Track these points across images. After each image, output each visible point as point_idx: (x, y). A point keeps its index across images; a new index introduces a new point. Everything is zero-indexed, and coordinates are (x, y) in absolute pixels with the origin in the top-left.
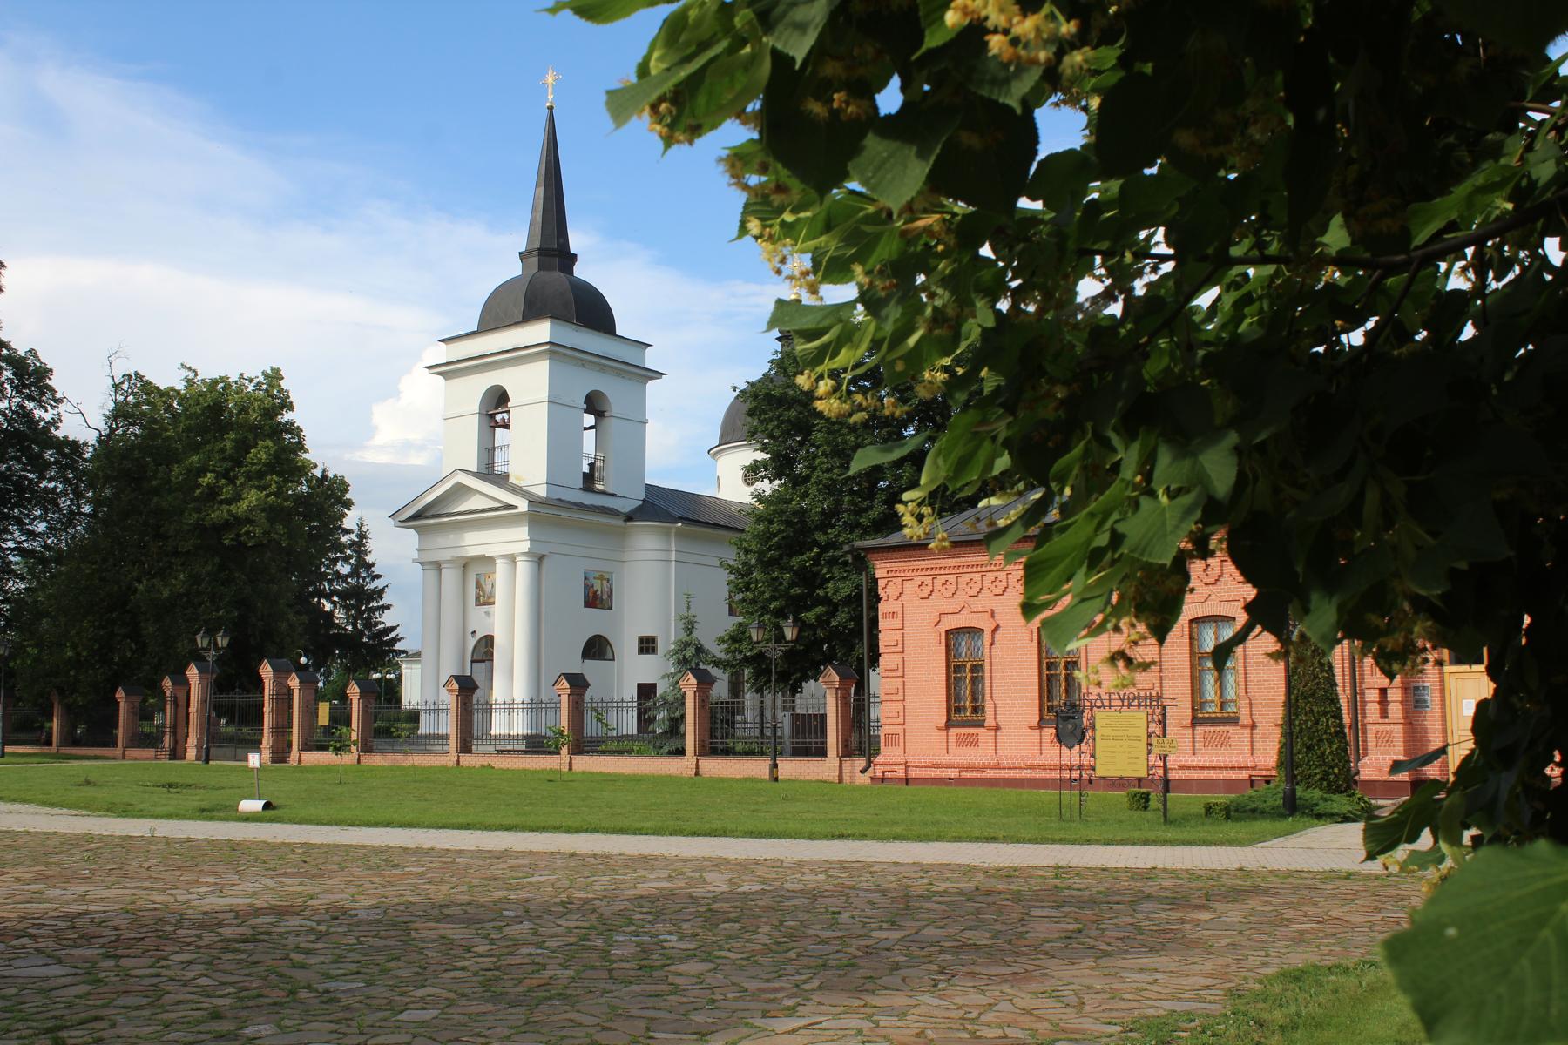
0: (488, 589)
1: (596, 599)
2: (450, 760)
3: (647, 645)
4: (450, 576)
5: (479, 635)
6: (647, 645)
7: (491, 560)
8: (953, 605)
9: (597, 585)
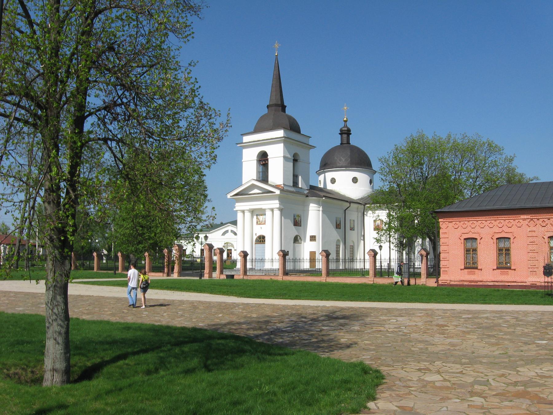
2: (241, 277)
3: (313, 238)
6: (313, 238)
7: (265, 210)
8: (466, 231)
9: (297, 219)
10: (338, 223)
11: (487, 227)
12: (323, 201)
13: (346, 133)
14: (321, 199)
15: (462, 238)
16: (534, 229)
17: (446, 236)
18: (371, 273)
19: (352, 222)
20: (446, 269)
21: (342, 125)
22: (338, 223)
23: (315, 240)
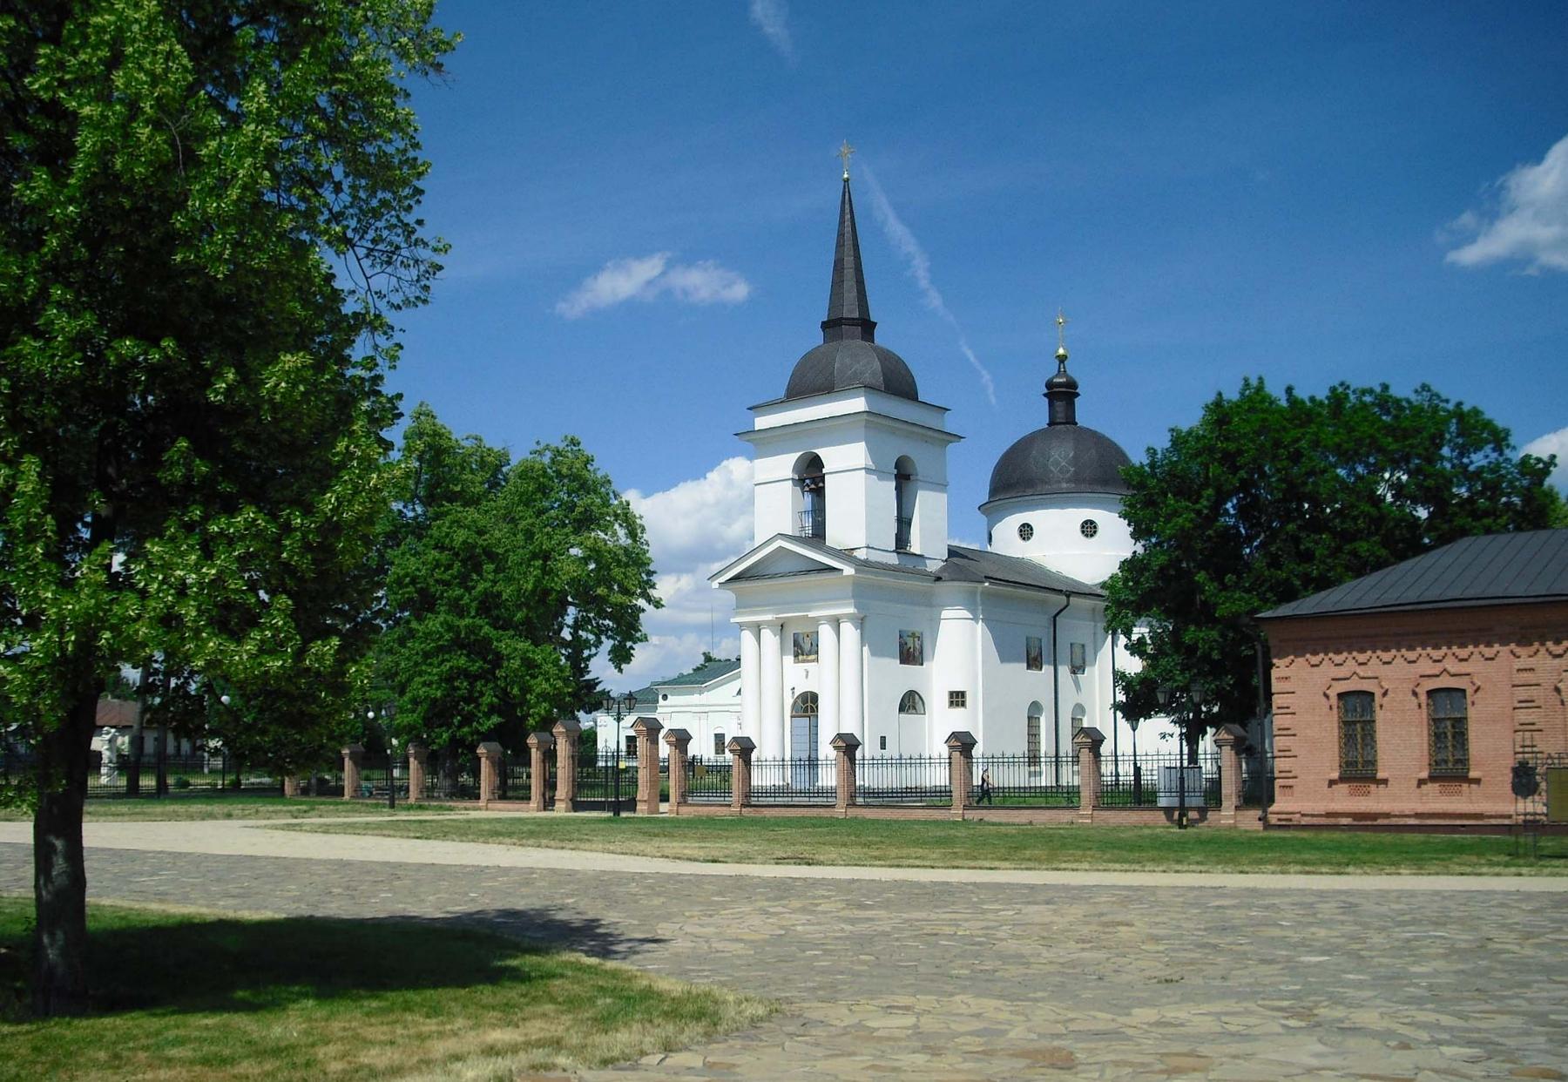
6: (957, 699)
7: (816, 621)
9: (910, 644)
11: (1399, 660)
12: (985, 593)
13: (1062, 395)
14: (979, 586)
15: (1333, 693)
16: (1531, 662)
18: (1086, 795)
19: (1078, 650)
21: (1050, 371)
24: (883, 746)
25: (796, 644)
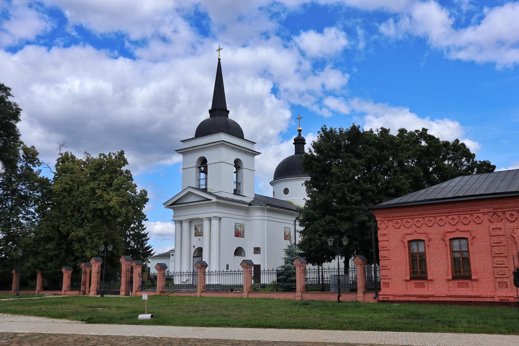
0: (199, 230)
1: (238, 234)
3: (257, 250)
4: (186, 225)
5: (196, 247)
6: (257, 250)
7: (201, 220)
8: (410, 231)
9: (239, 229)
10: (287, 234)
11: (436, 226)
16: (499, 225)
17: (385, 238)
20: (387, 281)
22: (287, 234)
23: (259, 253)
24: (227, 268)
25: (196, 229)
